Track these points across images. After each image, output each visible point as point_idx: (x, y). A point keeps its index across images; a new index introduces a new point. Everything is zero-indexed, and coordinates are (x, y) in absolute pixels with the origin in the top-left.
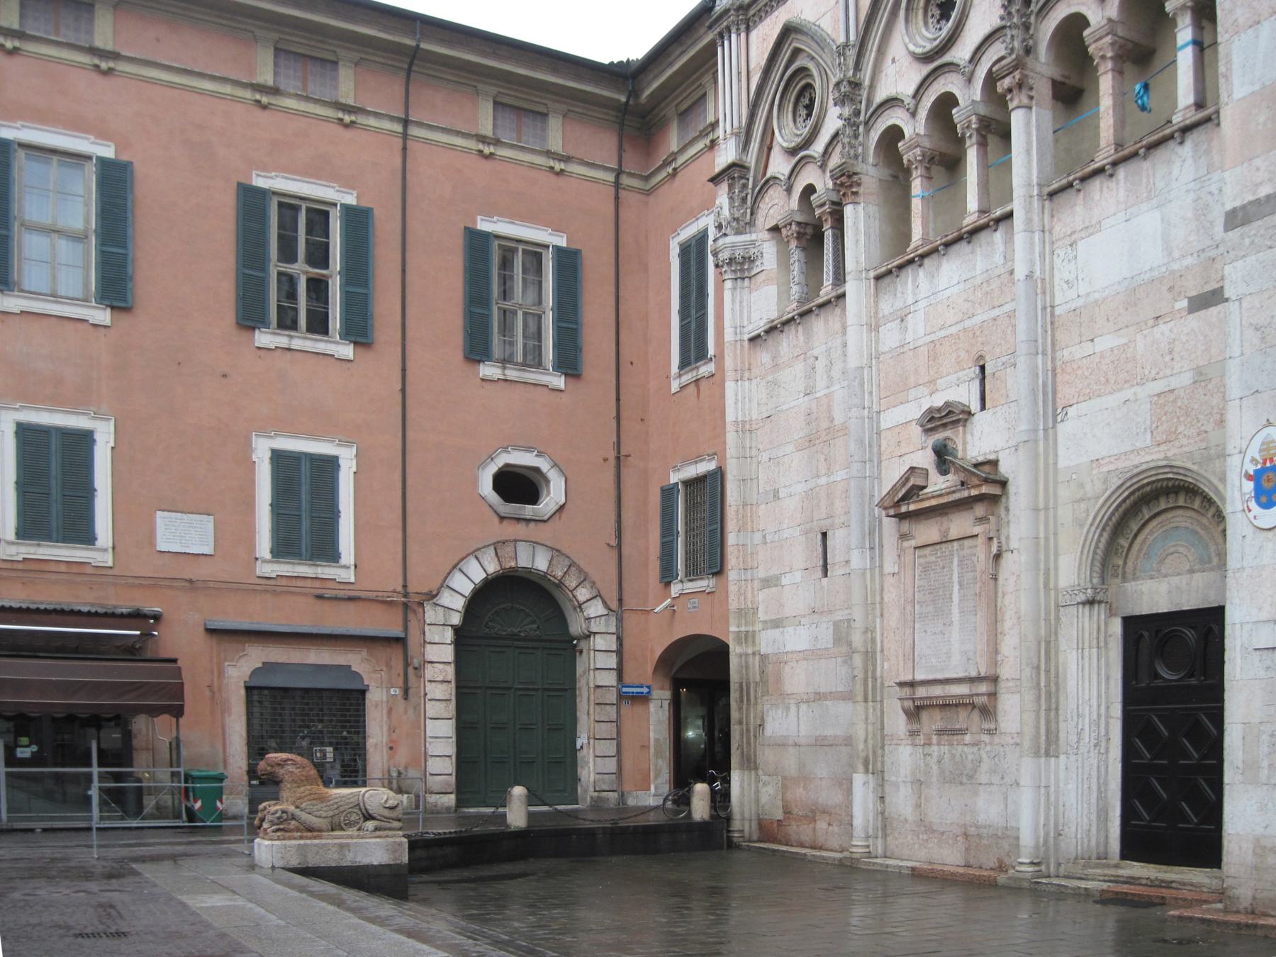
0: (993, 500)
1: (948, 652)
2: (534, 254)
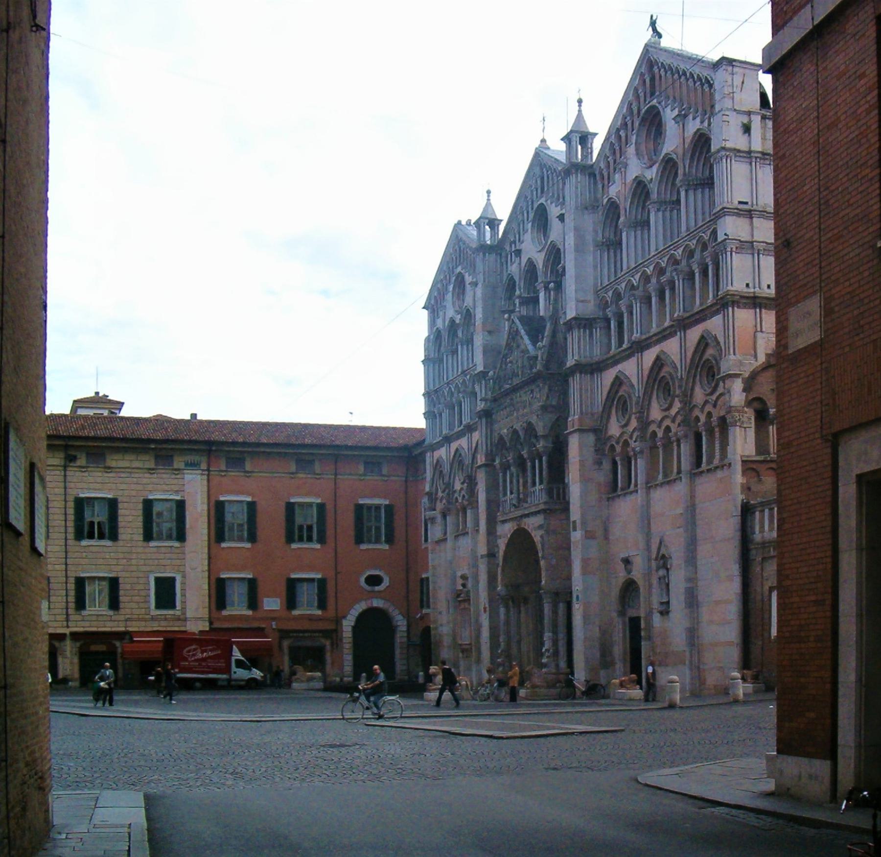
2: (378, 507)
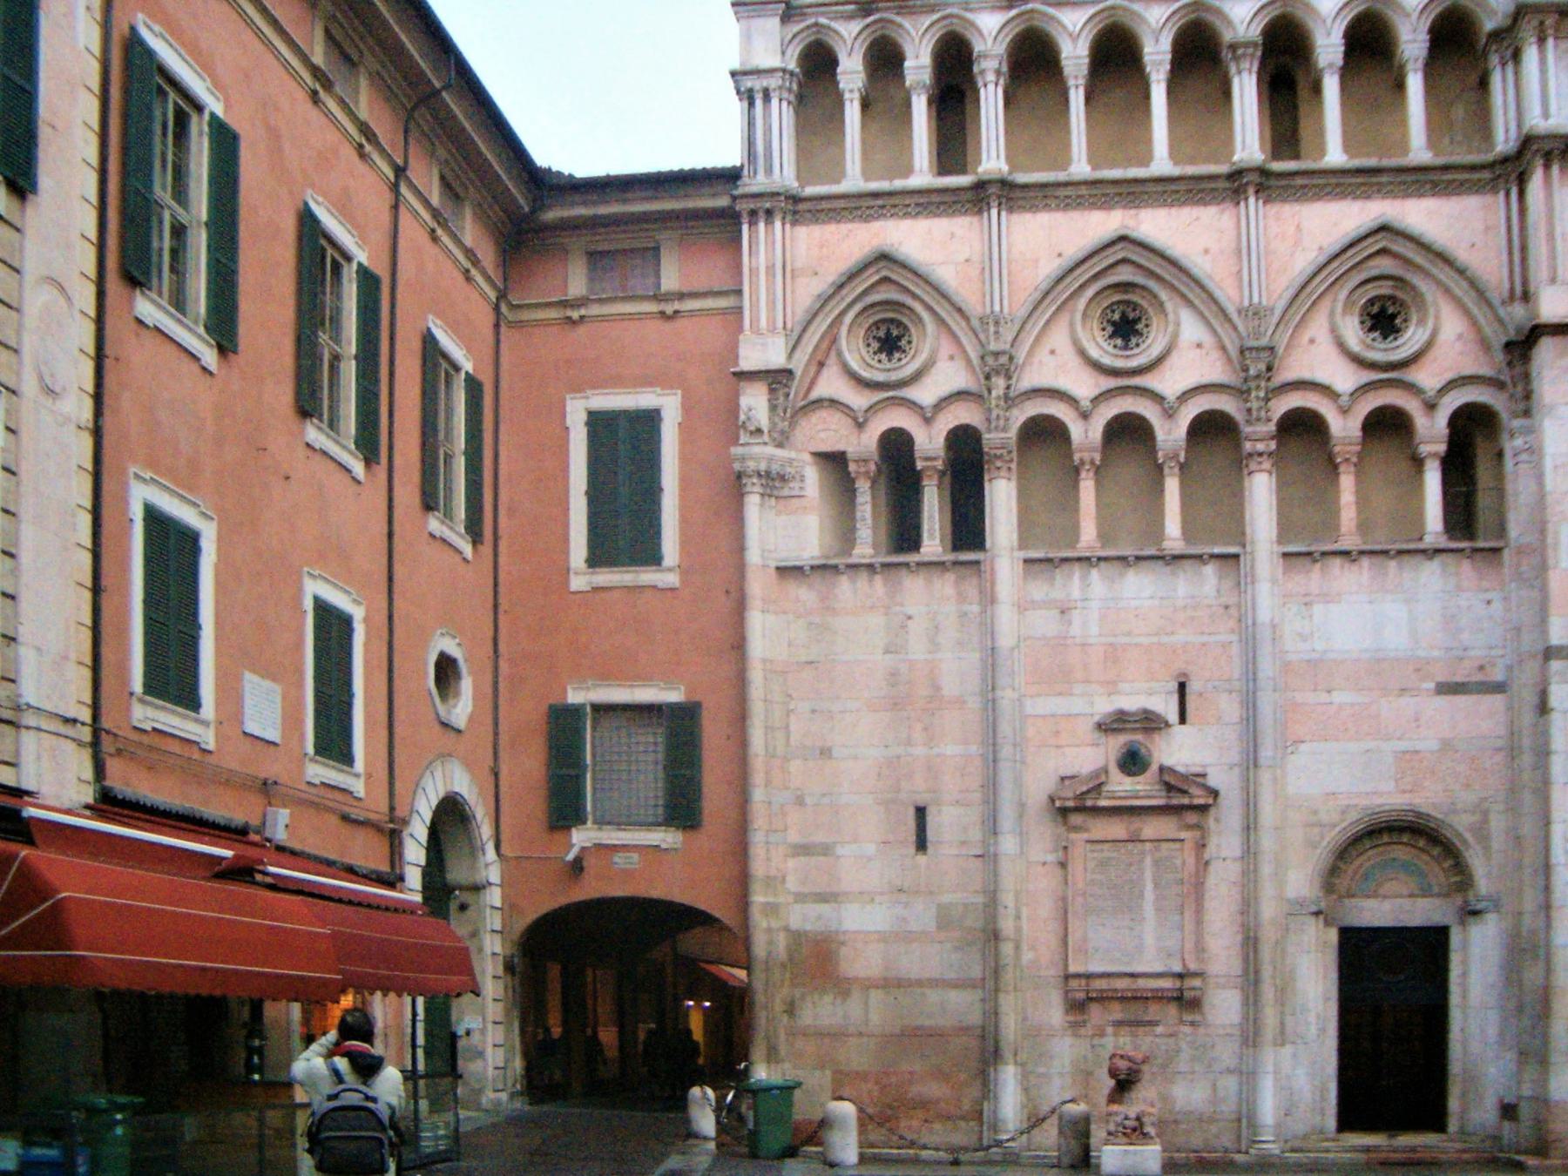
0: (1203, 809)
1: (1141, 945)
